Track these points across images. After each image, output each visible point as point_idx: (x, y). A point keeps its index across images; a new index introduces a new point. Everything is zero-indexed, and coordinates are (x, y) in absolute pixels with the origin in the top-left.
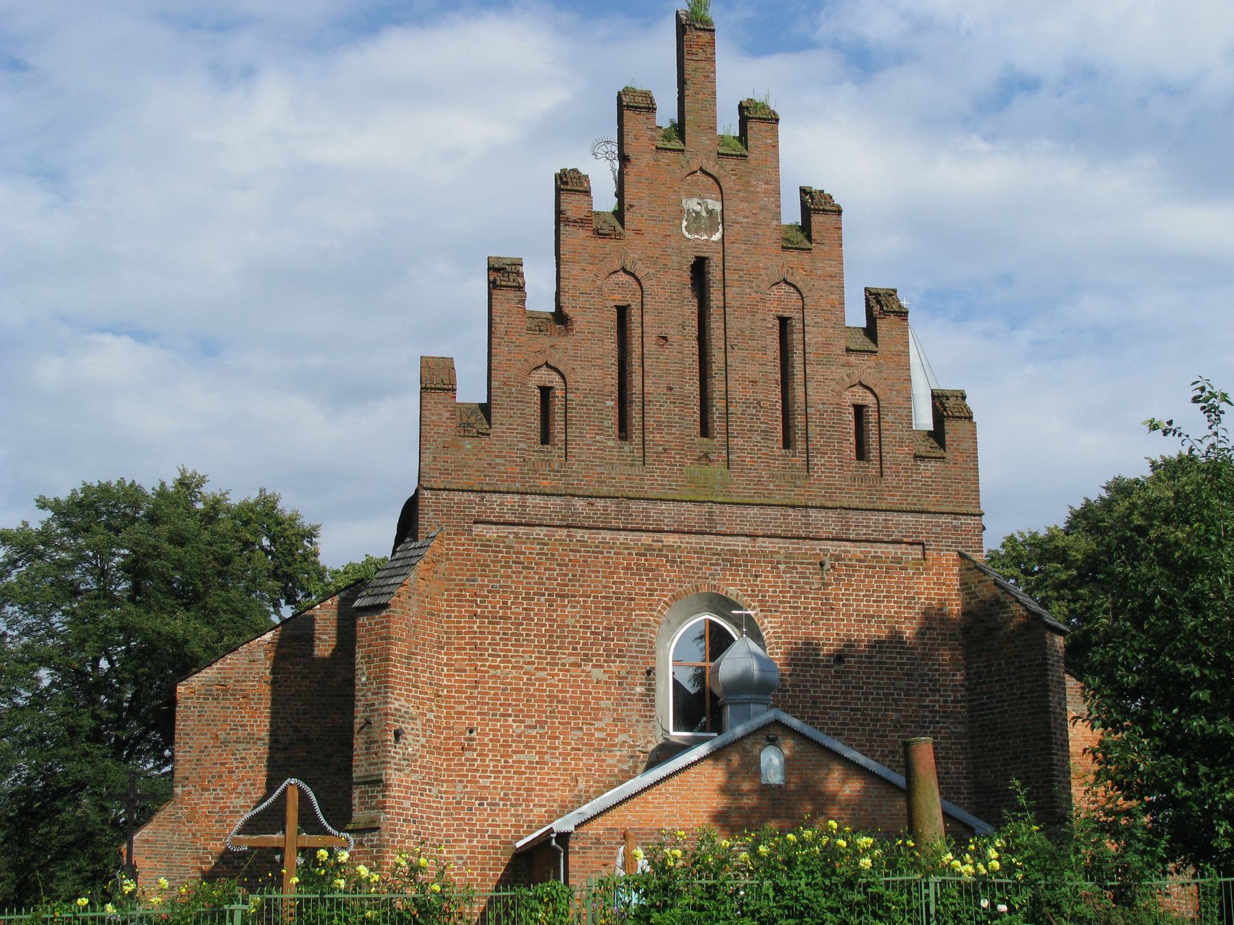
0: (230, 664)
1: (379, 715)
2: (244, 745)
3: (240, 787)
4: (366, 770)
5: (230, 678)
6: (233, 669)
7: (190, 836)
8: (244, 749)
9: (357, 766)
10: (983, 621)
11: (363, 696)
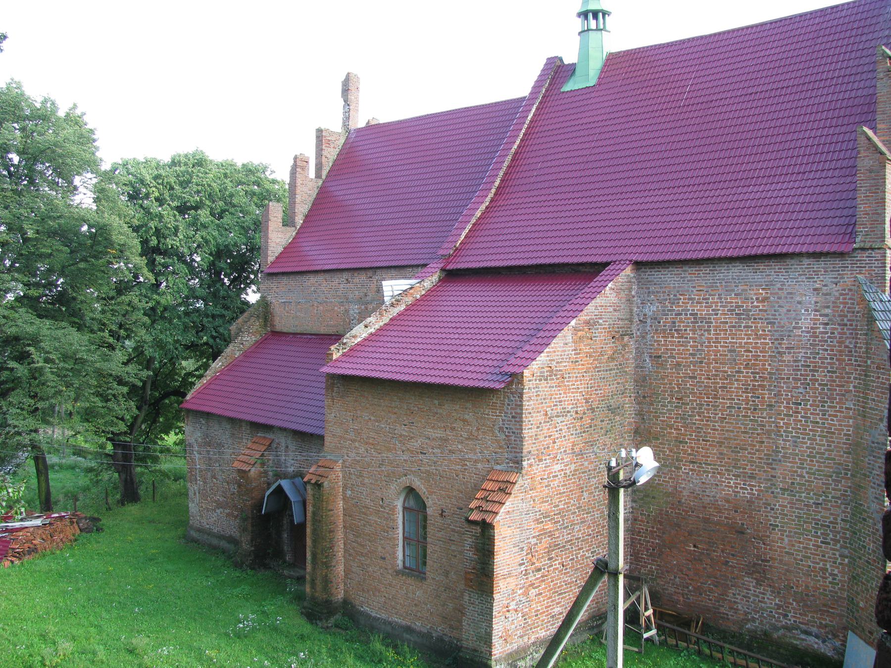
0: (553, 348)
2: (561, 419)
6: (555, 352)
7: (532, 502)
8: (561, 422)
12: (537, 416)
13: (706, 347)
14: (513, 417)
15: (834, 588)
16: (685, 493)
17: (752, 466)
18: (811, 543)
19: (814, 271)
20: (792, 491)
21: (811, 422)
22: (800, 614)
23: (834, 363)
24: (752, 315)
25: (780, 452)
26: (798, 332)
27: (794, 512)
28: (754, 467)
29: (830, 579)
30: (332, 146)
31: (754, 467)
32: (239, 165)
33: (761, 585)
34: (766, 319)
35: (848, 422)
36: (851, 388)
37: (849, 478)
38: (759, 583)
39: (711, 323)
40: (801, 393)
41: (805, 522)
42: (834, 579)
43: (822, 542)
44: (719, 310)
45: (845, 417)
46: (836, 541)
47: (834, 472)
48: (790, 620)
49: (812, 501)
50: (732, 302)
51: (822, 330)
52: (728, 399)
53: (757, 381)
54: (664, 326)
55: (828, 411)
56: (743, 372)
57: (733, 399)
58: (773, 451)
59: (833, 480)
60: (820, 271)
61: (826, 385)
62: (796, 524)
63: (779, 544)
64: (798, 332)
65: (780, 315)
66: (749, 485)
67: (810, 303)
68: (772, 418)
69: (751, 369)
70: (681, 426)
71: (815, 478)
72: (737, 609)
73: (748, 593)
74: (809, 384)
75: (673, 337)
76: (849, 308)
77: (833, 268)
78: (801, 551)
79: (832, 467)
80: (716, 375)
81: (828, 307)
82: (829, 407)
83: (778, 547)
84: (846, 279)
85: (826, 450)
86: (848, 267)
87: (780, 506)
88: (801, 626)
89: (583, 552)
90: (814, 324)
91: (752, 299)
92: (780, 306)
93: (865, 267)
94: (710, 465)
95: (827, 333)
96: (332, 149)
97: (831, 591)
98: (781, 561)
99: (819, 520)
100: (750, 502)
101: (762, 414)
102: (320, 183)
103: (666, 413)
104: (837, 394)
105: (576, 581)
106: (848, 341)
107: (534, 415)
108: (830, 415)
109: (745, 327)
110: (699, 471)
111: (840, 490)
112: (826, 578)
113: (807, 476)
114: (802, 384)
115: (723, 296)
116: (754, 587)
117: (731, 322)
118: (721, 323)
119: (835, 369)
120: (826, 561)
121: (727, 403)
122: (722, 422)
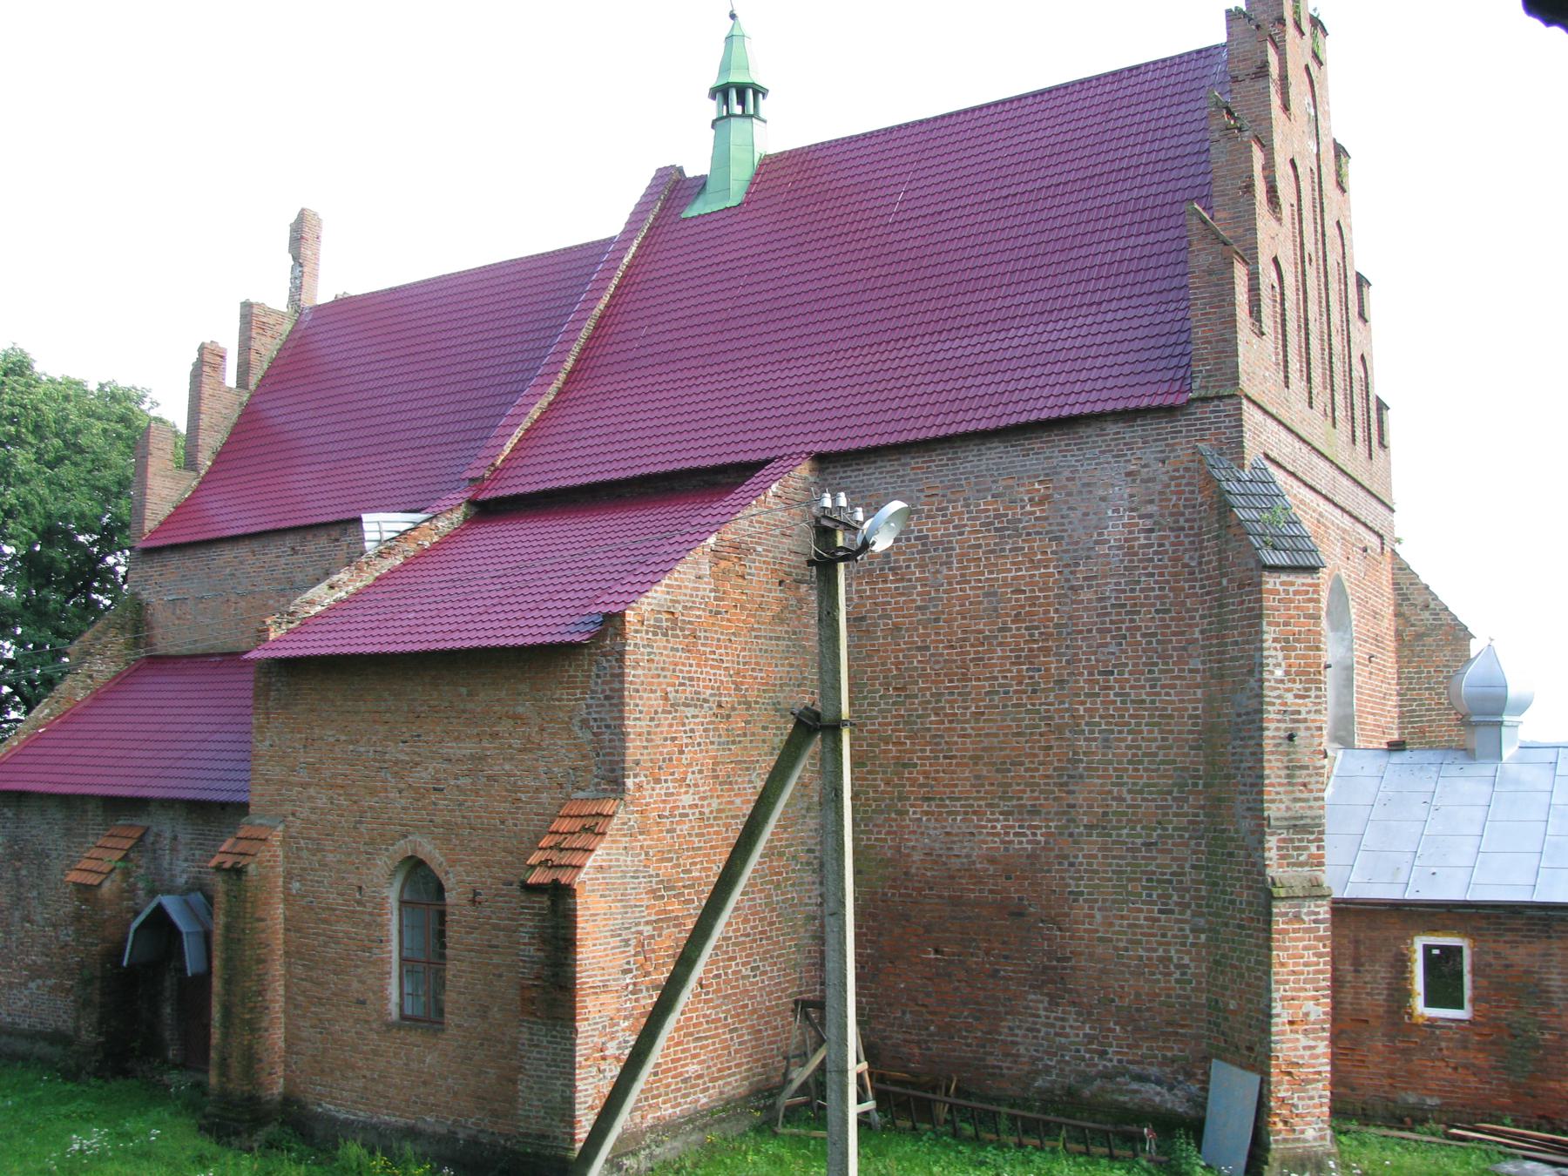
0: (676, 579)
1: (1308, 729)
3: (690, 776)
4: (1288, 808)
5: (678, 602)
7: (643, 857)
8: (693, 717)
9: (1273, 801)
10: (1412, 625)
11: (1279, 697)
12: (649, 699)
13: (945, 592)
14: (607, 698)
15: (1184, 989)
16: (917, 857)
17: (1032, 791)
18: (1142, 916)
19: (1125, 444)
20: (1104, 828)
21: (1133, 702)
22: (1129, 1046)
23: (1166, 596)
24: (1024, 528)
25: (1081, 761)
26: (1102, 550)
27: (1110, 865)
28: (1036, 794)
29: (1177, 975)
30: (269, 333)
31: (1036, 794)
32: (93, 387)
33: (1058, 1004)
34: (1047, 533)
35: (1195, 693)
36: (1197, 635)
37: (1200, 793)
38: (1053, 1002)
39: (953, 549)
40: (1113, 653)
41: (1130, 880)
42: (1183, 974)
43: (1160, 911)
44: (965, 526)
45: (1189, 686)
46: (1184, 906)
47: (1174, 785)
48: (1111, 1060)
49: (1139, 841)
50: (988, 510)
51: (1143, 541)
52: (986, 679)
53: (1035, 641)
54: (870, 564)
55: (1159, 679)
56: (1010, 629)
57: (996, 678)
58: (1069, 761)
59: (1174, 799)
60: (1136, 443)
61: (1154, 635)
62: (1114, 886)
63: (1087, 926)
64: (1102, 550)
65: (1070, 523)
66: (1030, 827)
67: (1121, 498)
68: (1064, 703)
69: (1024, 621)
70: (906, 737)
71: (1144, 800)
72: (1018, 1056)
73: (1035, 1023)
74: (1124, 637)
75: (885, 582)
76: (1186, 500)
77: (1158, 434)
78: (1125, 933)
79: (1170, 777)
80: (964, 640)
81: (1151, 502)
82: (1161, 672)
83: (1085, 930)
84: (1179, 452)
85: (1159, 748)
86: (1181, 432)
87: (1084, 856)
88: (1131, 1067)
89: (737, 965)
90: (1130, 532)
91: (1022, 500)
92: (1070, 509)
93: (1209, 429)
94: (959, 799)
95: (1151, 545)
96: (269, 340)
97: (1179, 996)
98: (1091, 955)
99: (1154, 873)
100: (1033, 856)
101: (1047, 697)
102: (245, 397)
103: (876, 717)
104: (1174, 649)
105: (726, 1018)
106: (1187, 556)
107: (645, 695)
108: (1163, 686)
109: (1011, 550)
110: (940, 813)
111: (1186, 814)
112: (1170, 974)
113: (1128, 797)
114: (1113, 638)
115: (971, 501)
116: (1046, 1009)
117: (988, 545)
118: (969, 547)
119: (1168, 606)
120: (1169, 944)
121: (984, 687)
122: (977, 721)
